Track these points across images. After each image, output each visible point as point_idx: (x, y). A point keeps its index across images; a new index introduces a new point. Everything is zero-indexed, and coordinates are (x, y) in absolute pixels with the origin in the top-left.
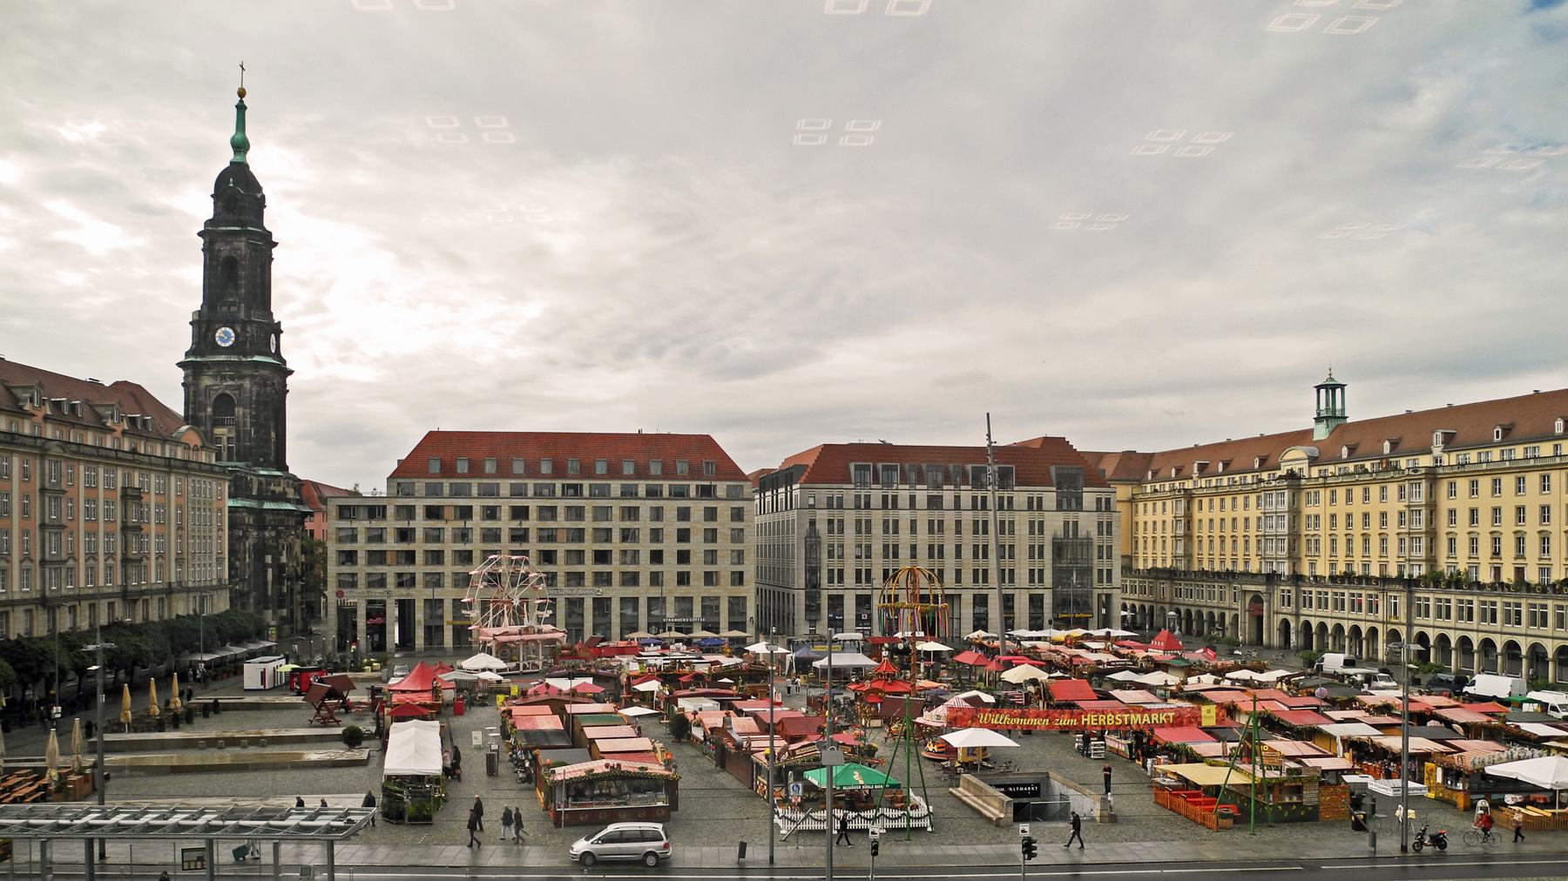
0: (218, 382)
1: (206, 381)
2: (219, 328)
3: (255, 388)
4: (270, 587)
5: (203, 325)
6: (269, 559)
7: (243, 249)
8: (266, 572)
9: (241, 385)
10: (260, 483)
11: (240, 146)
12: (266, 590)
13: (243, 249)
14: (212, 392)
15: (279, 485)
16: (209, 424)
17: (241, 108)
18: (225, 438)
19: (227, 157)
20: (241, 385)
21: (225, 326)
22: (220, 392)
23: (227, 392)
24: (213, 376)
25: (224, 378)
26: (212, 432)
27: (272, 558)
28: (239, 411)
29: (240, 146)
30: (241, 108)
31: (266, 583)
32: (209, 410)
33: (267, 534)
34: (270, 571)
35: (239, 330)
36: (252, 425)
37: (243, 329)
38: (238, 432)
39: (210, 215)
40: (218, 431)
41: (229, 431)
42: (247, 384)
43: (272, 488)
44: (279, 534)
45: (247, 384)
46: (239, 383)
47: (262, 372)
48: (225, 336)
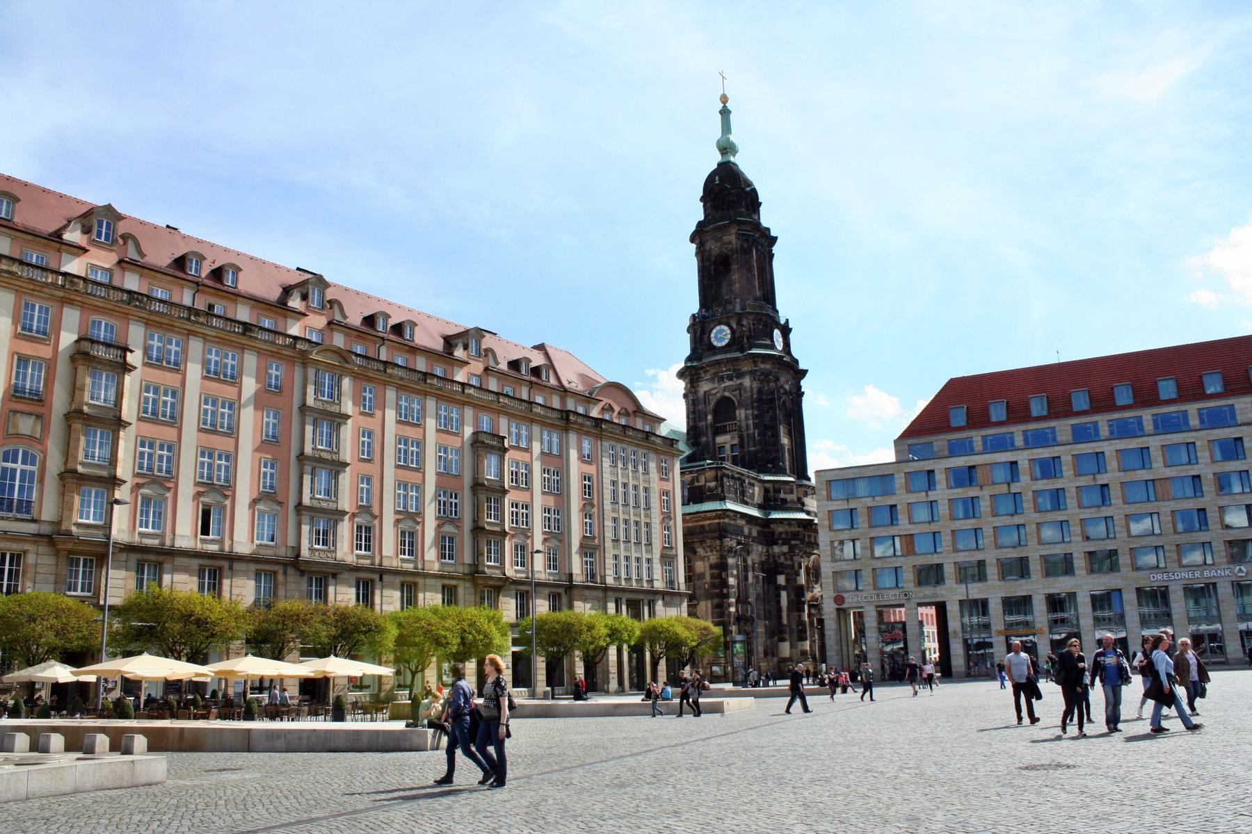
0: (716, 385)
1: (705, 387)
2: (712, 329)
3: (755, 385)
4: (784, 614)
5: (699, 328)
6: (781, 580)
7: (734, 242)
8: (779, 596)
9: (741, 384)
10: (766, 491)
11: (726, 148)
12: (780, 617)
13: (734, 242)
14: (711, 397)
15: (792, 492)
16: (710, 435)
17: (725, 113)
18: (728, 447)
19: (712, 160)
20: (741, 384)
21: (720, 324)
22: (719, 395)
23: (727, 394)
24: (712, 380)
25: (721, 379)
26: (714, 440)
27: (787, 580)
28: (741, 413)
29: (726, 148)
30: (725, 113)
31: (779, 610)
32: (710, 417)
33: (776, 549)
34: (784, 594)
35: (734, 326)
36: (755, 426)
37: (739, 323)
38: (741, 437)
39: (702, 218)
40: (720, 439)
41: (732, 438)
42: (747, 382)
43: (782, 495)
44: (792, 548)
45: (747, 382)
46: (738, 382)
47: (762, 366)
48: (721, 335)
